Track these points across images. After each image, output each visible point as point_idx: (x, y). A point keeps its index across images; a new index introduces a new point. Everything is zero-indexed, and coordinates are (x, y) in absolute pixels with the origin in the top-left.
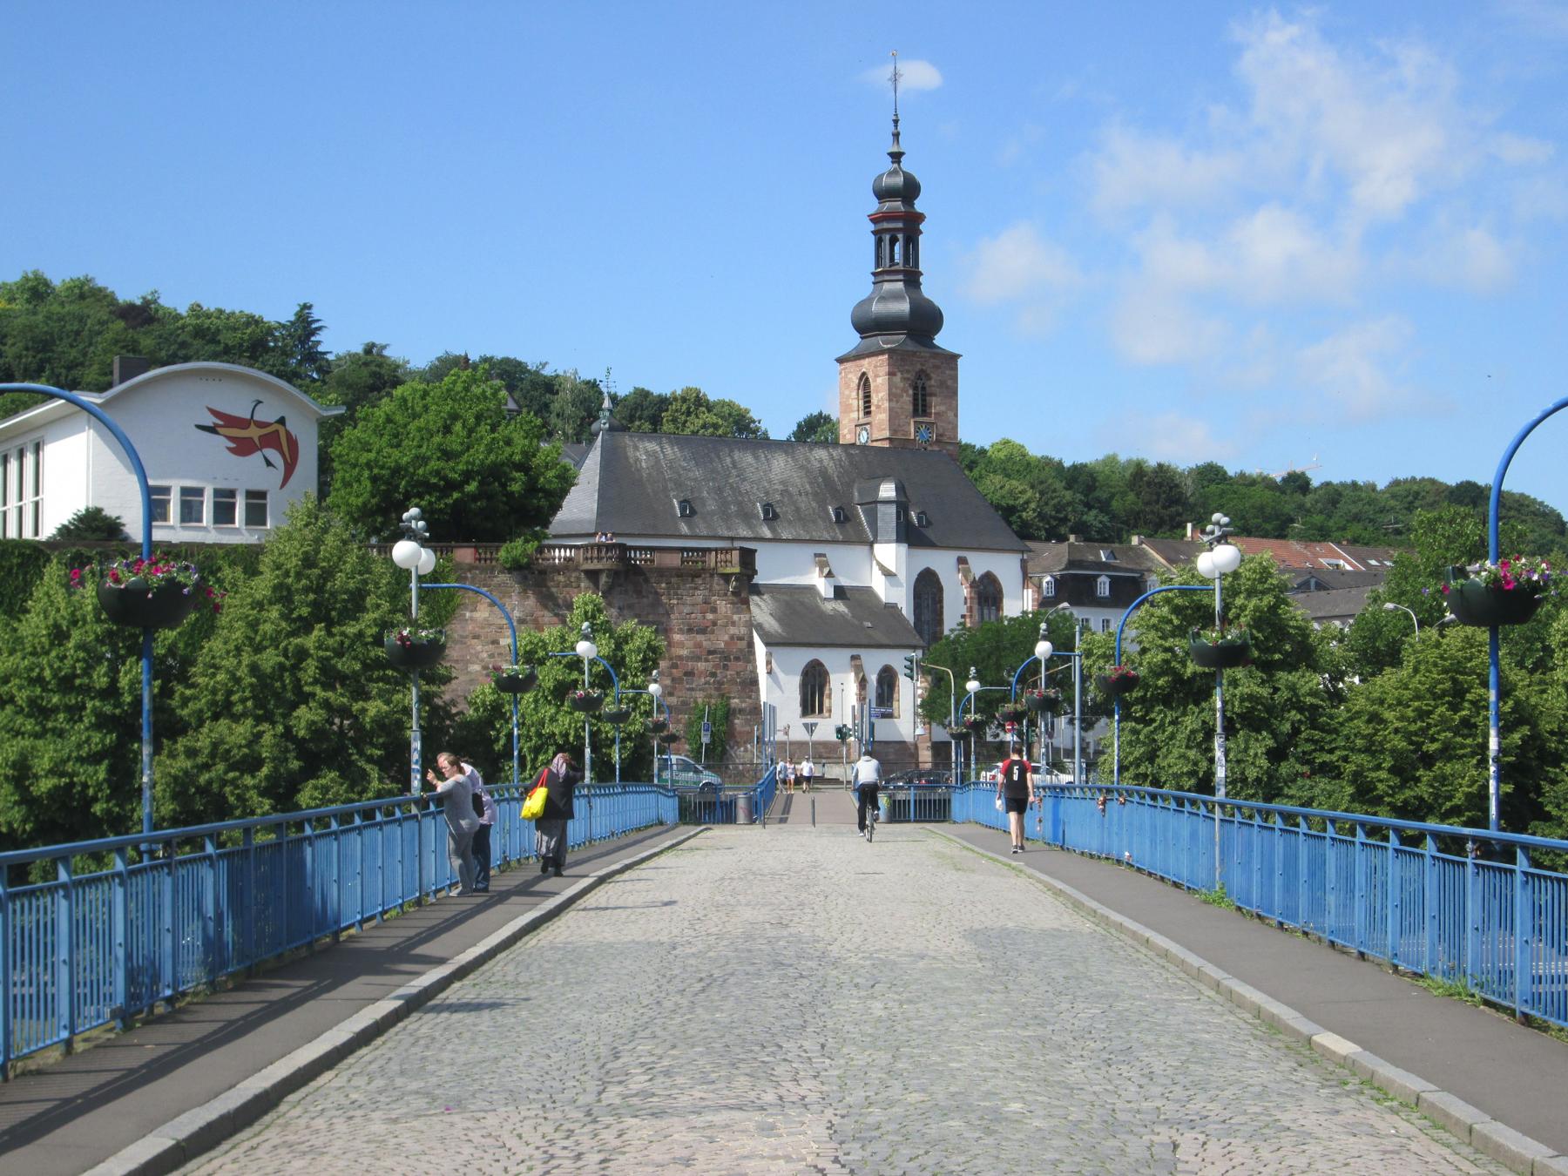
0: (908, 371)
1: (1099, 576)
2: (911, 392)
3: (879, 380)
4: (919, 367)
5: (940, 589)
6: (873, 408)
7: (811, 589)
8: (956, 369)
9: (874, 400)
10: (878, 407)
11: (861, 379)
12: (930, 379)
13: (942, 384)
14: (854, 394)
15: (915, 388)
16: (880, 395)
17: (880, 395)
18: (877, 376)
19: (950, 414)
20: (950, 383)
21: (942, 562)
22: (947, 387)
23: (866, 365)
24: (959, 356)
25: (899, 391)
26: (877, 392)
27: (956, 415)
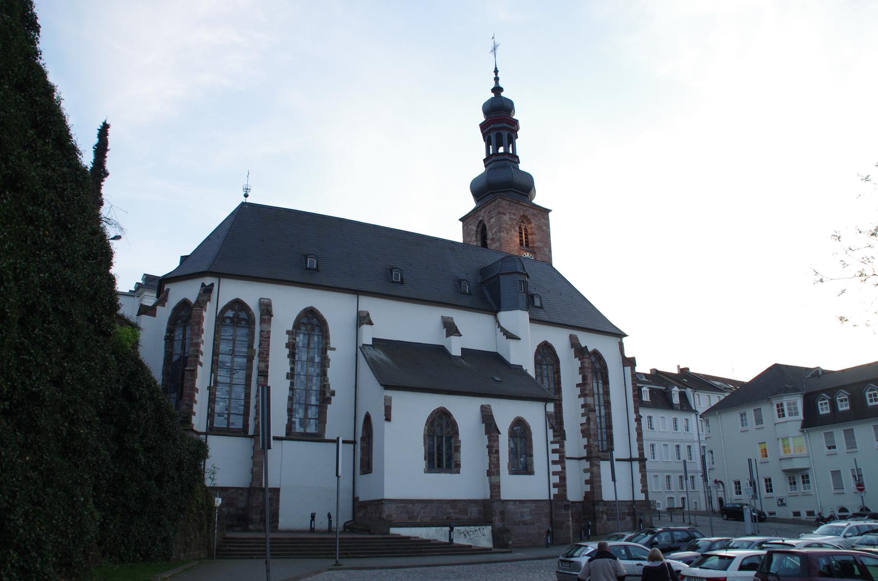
0: (514, 214)
1: (643, 387)
2: (517, 229)
3: (493, 220)
4: (522, 213)
5: (557, 361)
6: (489, 242)
7: (441, 351)
8: (547, 219)
9: (490, 235)
10: (493, 239)
11: (478, 227)
12: (530, 223)
13: (539, 227)
14: (474, 238)
15: (520, 228)
16: (494, 231)
17: (494, 231)
18: (491, 218)
19: (546, 249)
20: (544, 228)
21: (559, 340)
22: (543, 231)
23: (482, 215)
24: (550, 211)
25: (508, 227)
26: (491, 229)
27: (550, 251)
